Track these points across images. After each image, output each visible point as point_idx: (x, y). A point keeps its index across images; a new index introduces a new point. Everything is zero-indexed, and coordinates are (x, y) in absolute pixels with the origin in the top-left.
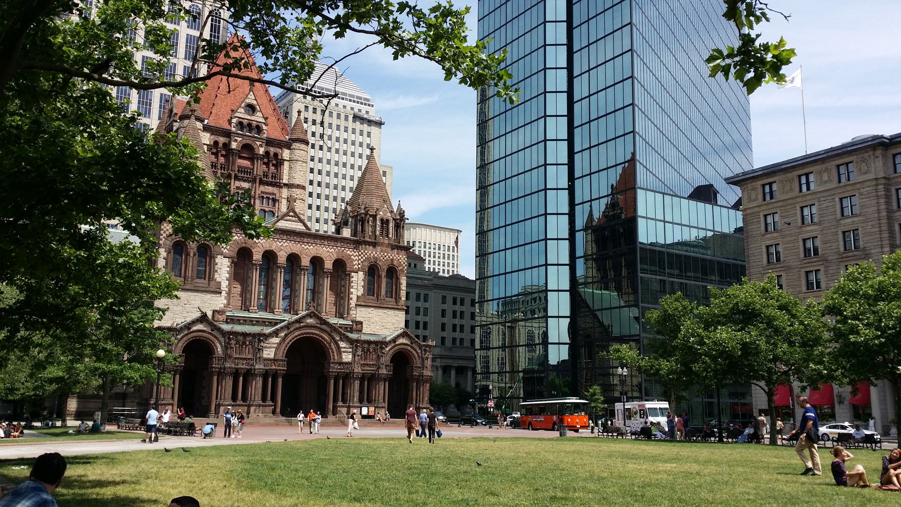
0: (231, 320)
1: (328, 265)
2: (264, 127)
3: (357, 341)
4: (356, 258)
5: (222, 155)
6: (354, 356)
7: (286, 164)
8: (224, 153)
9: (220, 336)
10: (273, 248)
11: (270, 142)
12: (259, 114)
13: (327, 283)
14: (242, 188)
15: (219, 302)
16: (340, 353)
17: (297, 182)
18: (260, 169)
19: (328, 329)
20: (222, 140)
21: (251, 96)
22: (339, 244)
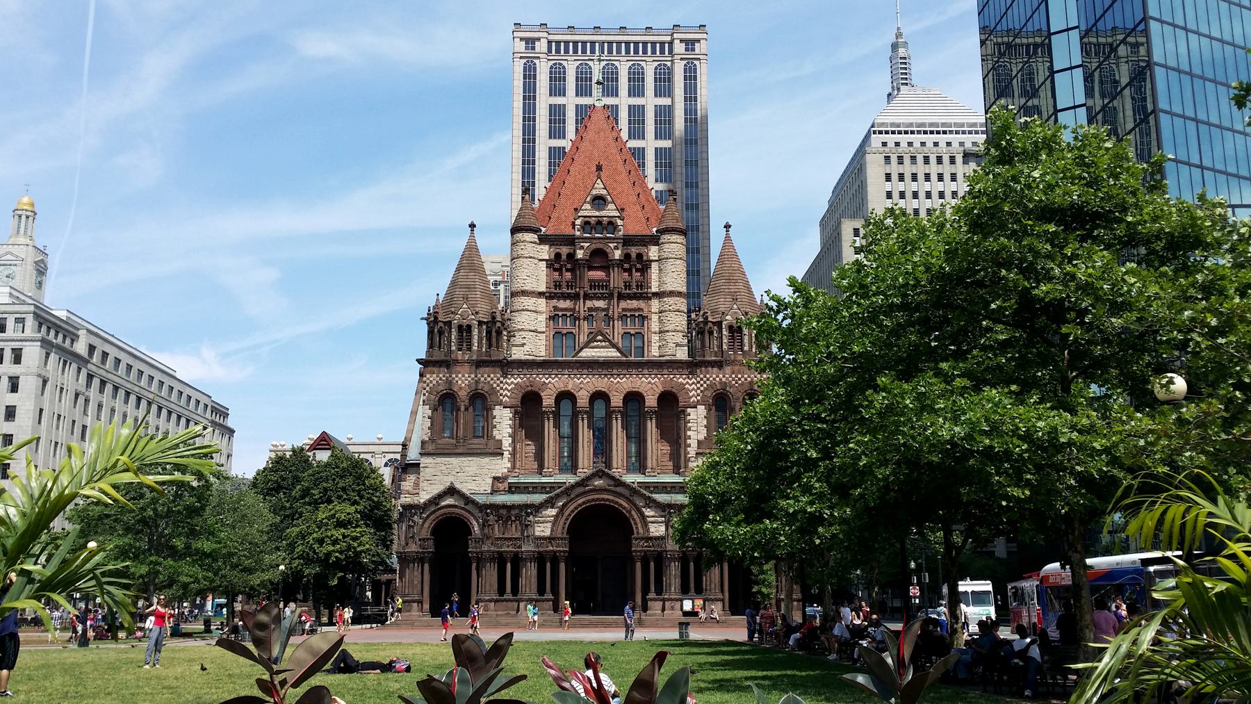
0: (514, 489)
1: (651, 401)
2: (619, 222)
3: (670, 506)
4: (693, 387)
5: (567, 270)
6: (667, 529)
7: (654, 266)
8: (569, 266)
9: (476, 512)
10: (570, 387)
11: (628, 241)
12: (611, 206)
13: (651, 426)
14: (597, 309)
15: (501, 466)
16: (645, 524)
17: (669, 288)
18: (617, 279)
19: (627, 493)
20: (565, 250)
21: (599, 185)
22: (665, 371)
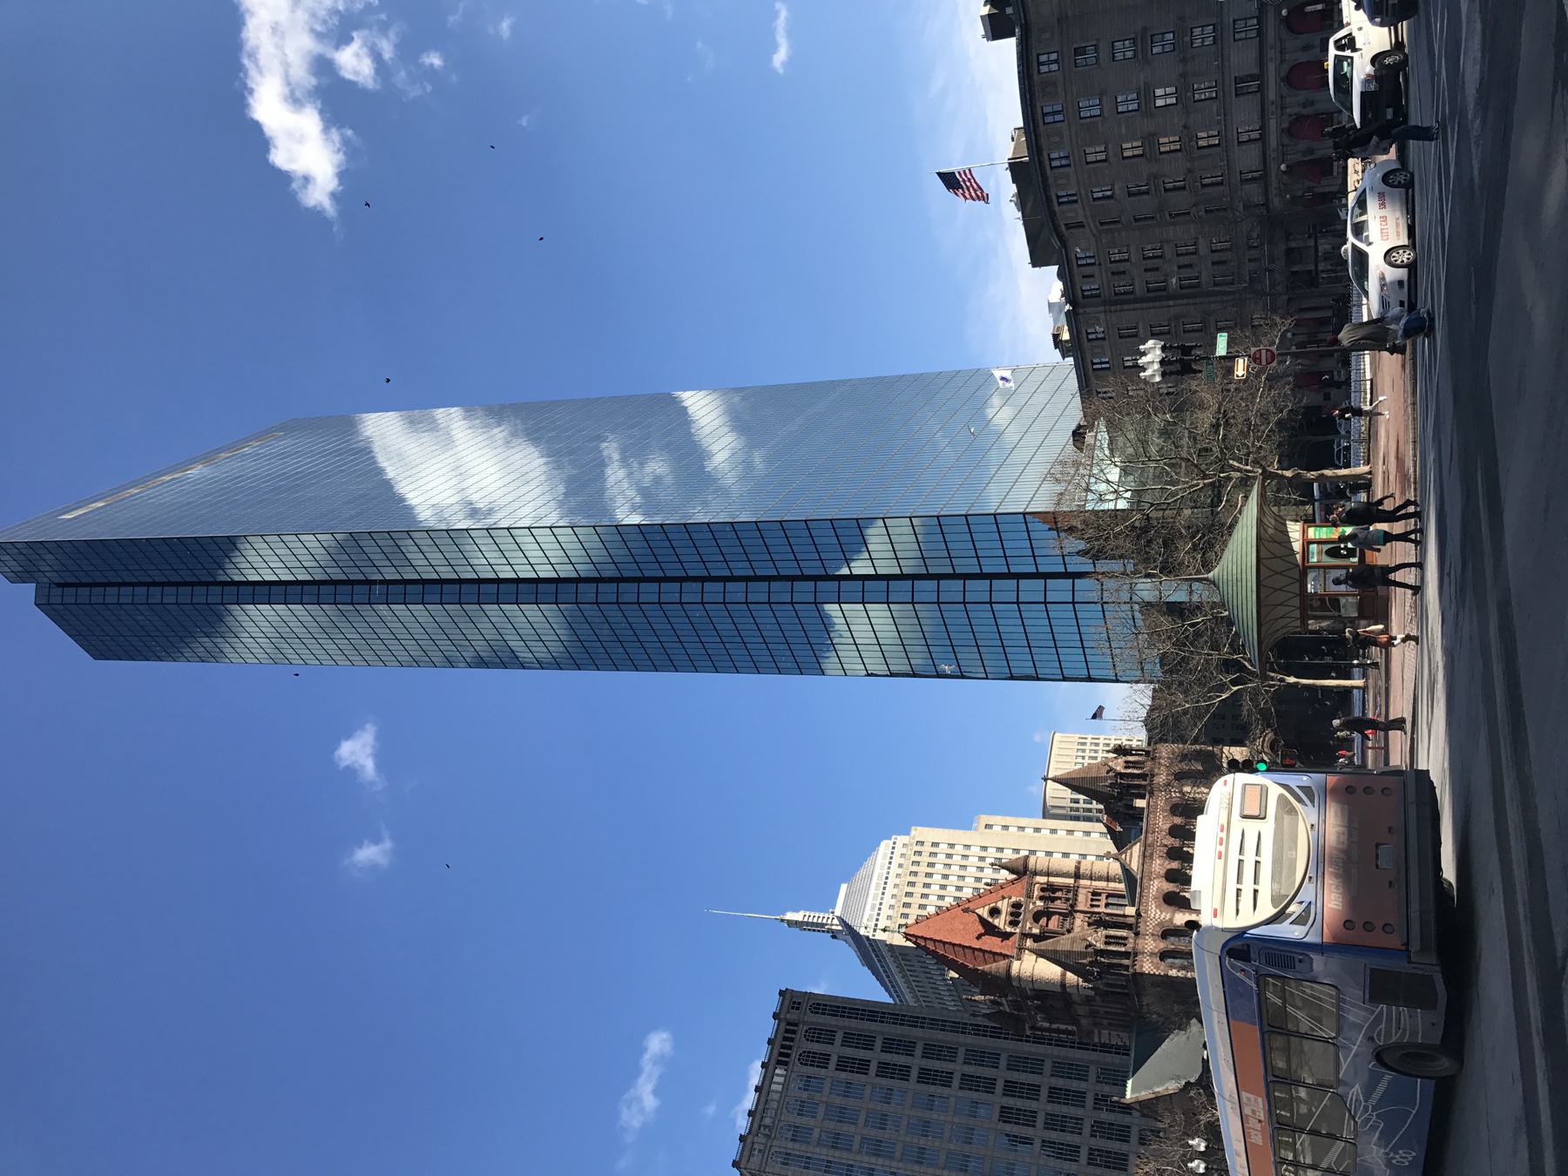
7: (1052, 879)
21: (979, 911)
